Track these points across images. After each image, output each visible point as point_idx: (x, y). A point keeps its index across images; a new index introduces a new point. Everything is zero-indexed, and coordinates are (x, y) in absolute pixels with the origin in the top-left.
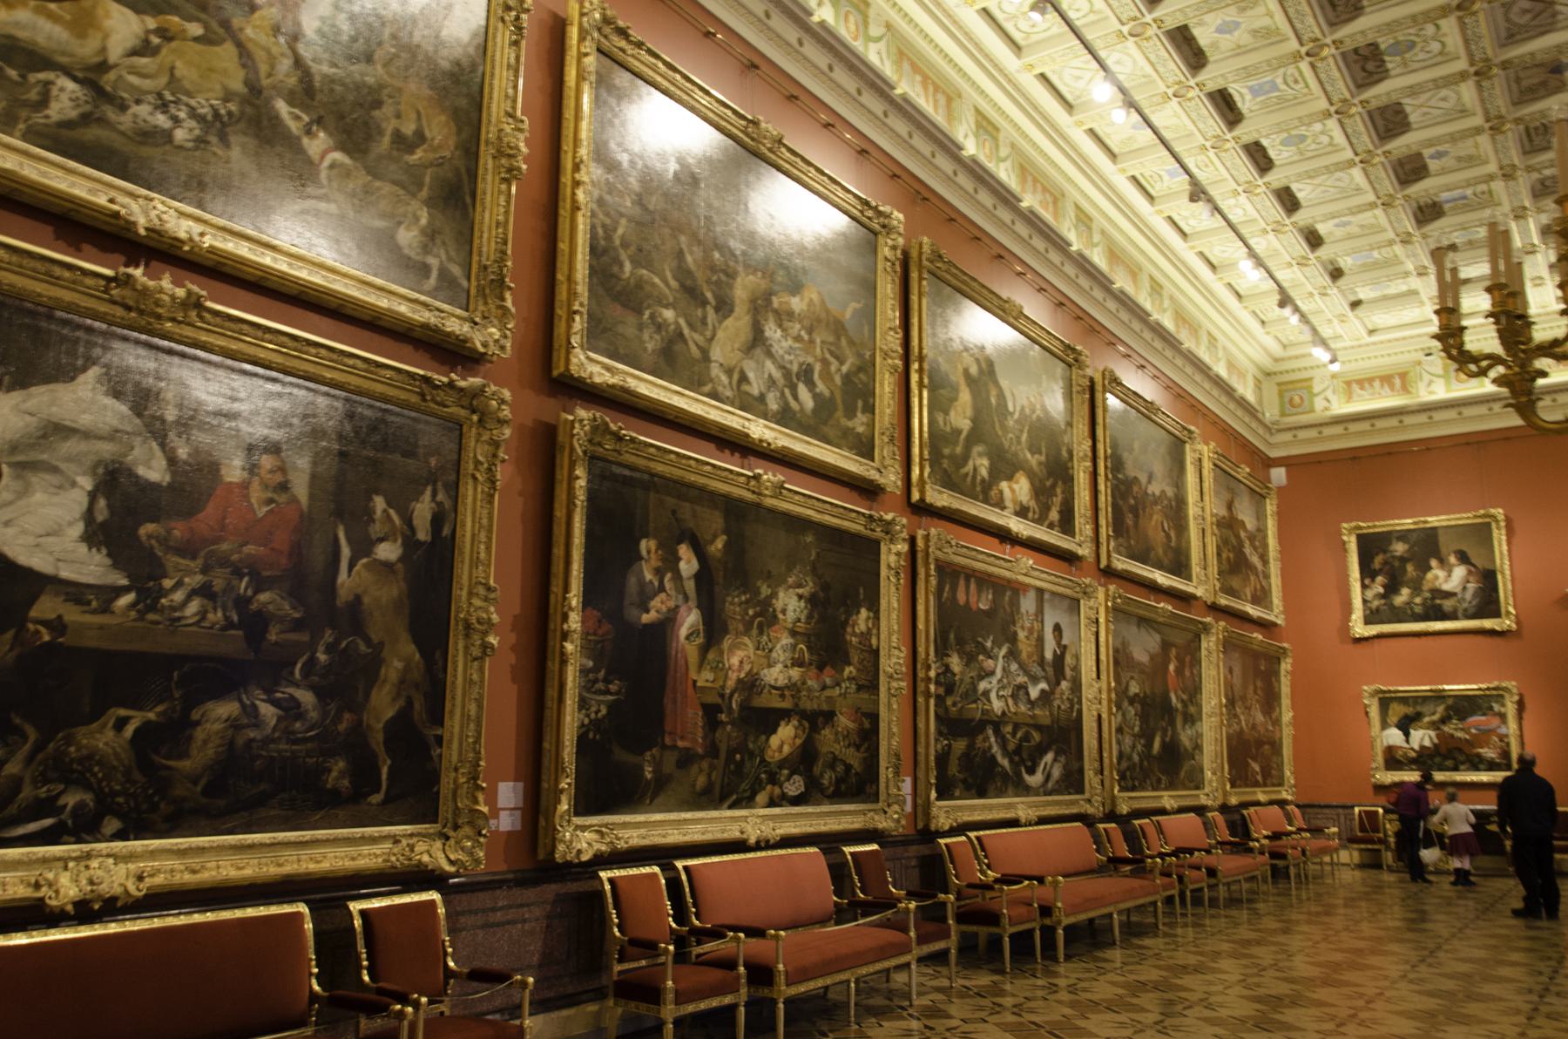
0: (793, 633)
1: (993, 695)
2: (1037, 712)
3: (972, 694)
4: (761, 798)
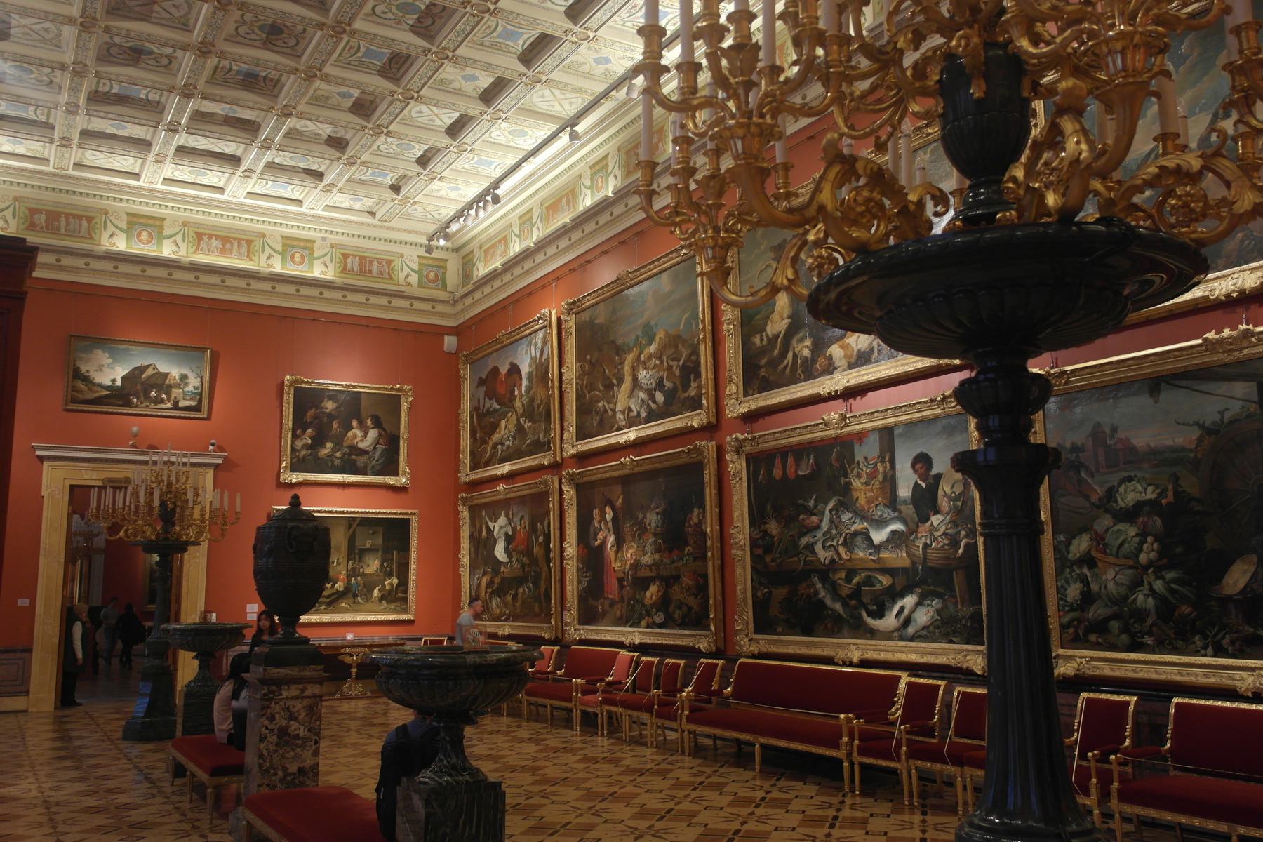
0: (655, 535)
1: (818, 548)
2: (885, 555)
3: (793, 548)
4: (643, 623)
